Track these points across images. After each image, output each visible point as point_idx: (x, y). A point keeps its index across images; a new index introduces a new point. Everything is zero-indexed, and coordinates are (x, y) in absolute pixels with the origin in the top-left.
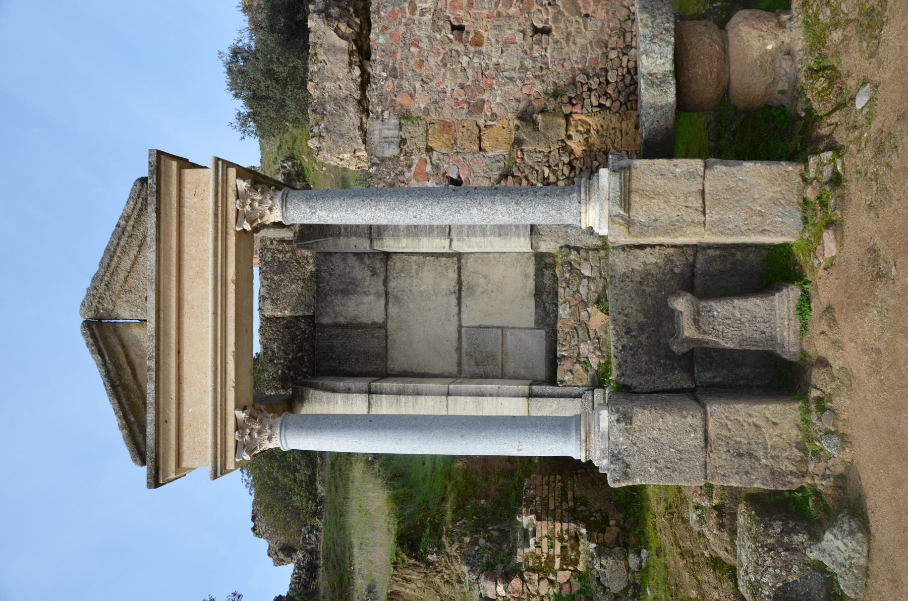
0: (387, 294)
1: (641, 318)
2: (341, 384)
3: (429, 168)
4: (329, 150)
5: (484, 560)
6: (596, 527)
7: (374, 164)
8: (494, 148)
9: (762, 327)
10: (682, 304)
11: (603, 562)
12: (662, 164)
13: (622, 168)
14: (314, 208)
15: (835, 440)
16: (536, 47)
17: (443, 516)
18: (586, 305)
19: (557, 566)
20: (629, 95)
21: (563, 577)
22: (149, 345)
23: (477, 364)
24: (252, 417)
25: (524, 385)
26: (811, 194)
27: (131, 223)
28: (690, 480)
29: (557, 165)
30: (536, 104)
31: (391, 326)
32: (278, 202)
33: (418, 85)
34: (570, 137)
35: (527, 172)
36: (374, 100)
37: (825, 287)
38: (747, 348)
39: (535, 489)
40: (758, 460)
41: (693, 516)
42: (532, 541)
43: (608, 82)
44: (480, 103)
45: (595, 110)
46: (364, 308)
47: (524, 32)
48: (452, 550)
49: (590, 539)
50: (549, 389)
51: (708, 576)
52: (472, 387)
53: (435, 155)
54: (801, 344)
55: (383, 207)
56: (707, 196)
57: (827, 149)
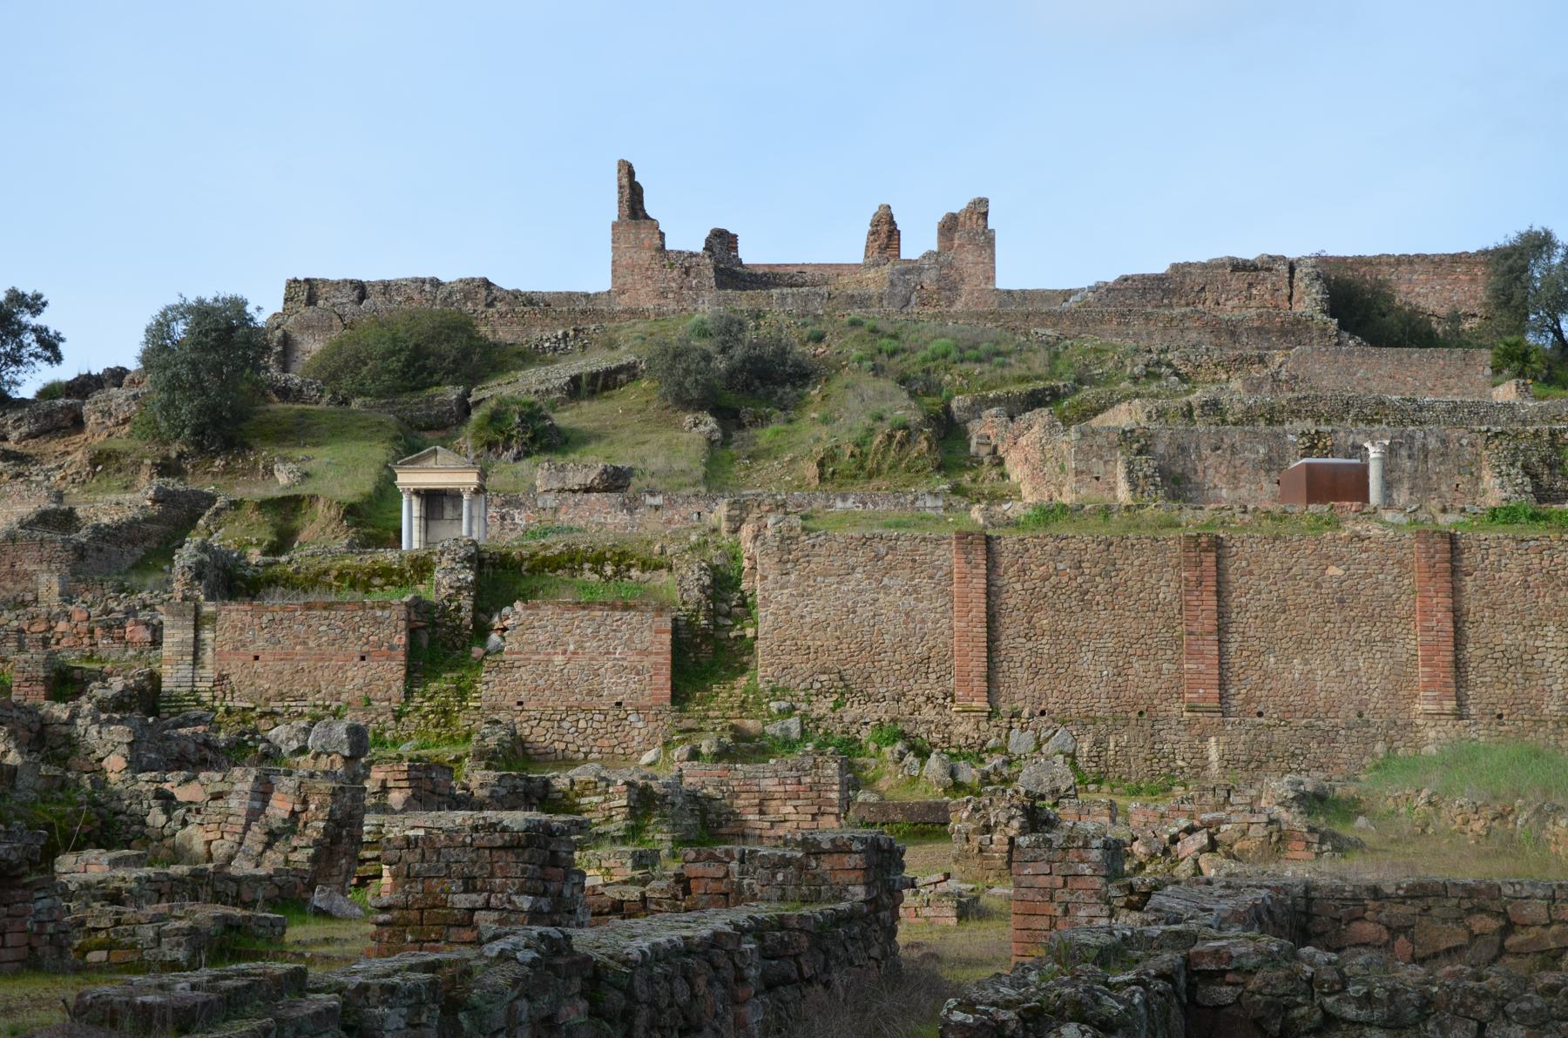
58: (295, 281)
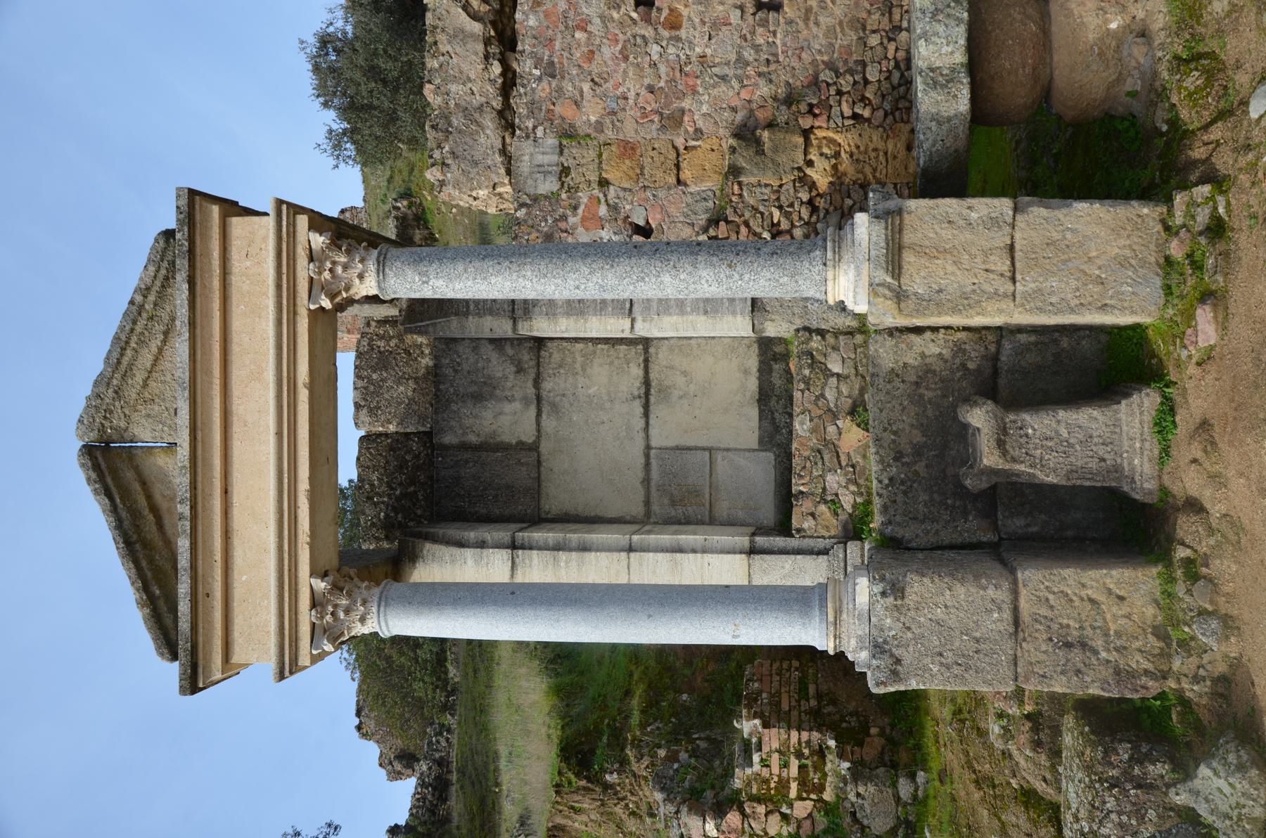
0: (539, 399)
1: (918, 437)
2: (472, 535)
3: (603, 211)
4: (457, 185)
5: (687, 784)
6: (850, 739)
7: (522, 205)
8: (698, 179)
9: (1101, 450)
10: (979, 417)
11: (861, 790)
12: (949, 205)
13: (888, 213)
14: (426, 274)
15: (1214, 624)
16: (760, 30)
17: (627, 717)
18: (835, 417)
19: (793, 793)
20: (897, 101)
21: (802, 809)
22: (181, 482)
23: (673, 503)
24: (336, 588)
25: (742, 535)
26: (1176, 250)
27: (152, 298)
28: (992, 683)
29: (792, 205)
30: (760, 115)
31: (545, 447)
32: (372, 267)
33: (586, 87)
34: (810, 163)
35: (747, 215)
36: (522, 111)
37: (1199, 395)
38: (1079, 482)
39: (761, 680)
40: (1096, 652)
41: (995, 729)
42: (756, 758)
43: (866, 82)
44: (677, 114)
45: (848, 122)
46: (505, 420)
47: (741, 8)
48: (640, 767)
49: (841, 755)
50: (780, 541)
51: (1016, 817)
52: (665, 538)
53: (612, 192)
54: (1160, 477)
55: (529, 273)
56: (1018, 255)
57: (1202, 181)
58: (359, 728)
